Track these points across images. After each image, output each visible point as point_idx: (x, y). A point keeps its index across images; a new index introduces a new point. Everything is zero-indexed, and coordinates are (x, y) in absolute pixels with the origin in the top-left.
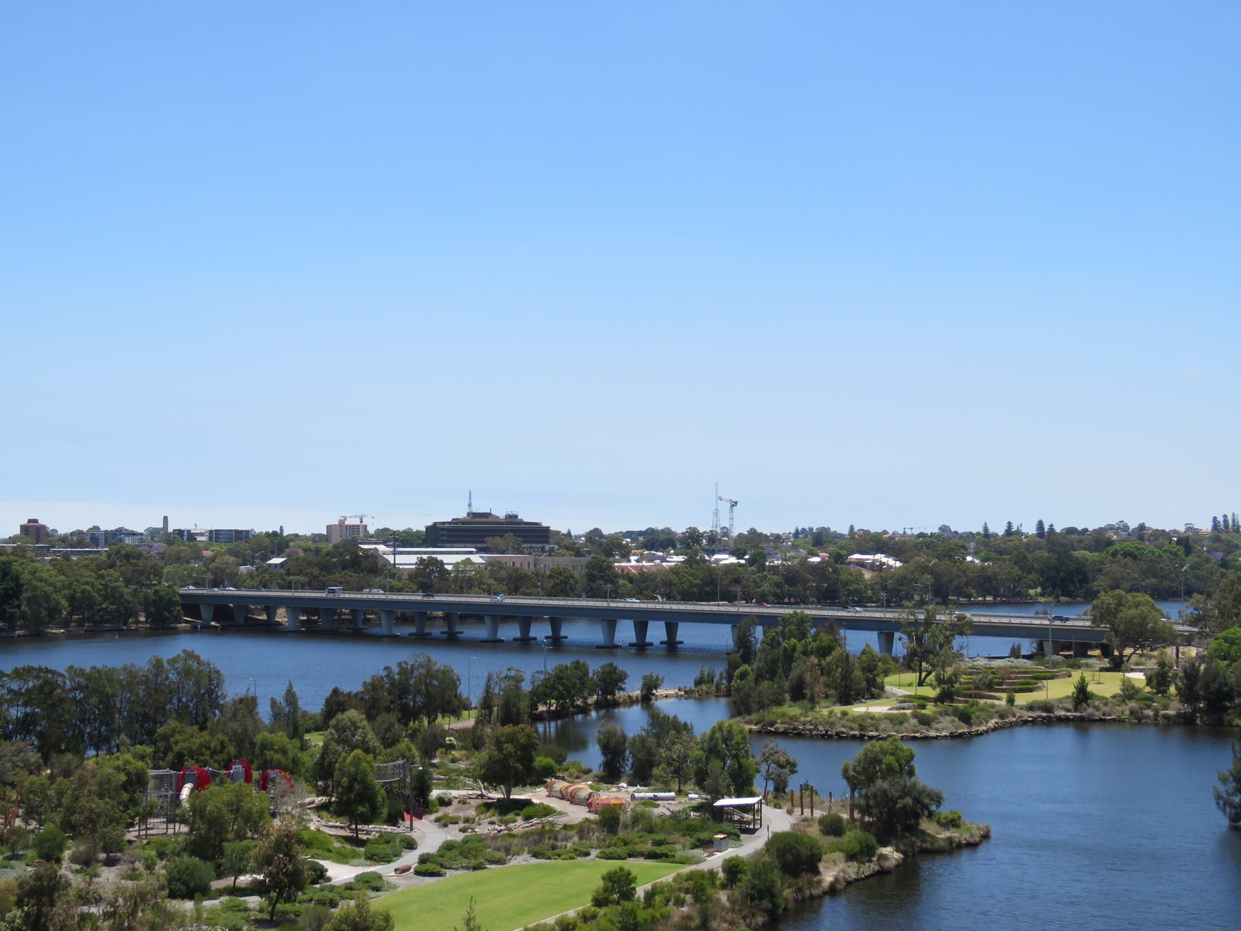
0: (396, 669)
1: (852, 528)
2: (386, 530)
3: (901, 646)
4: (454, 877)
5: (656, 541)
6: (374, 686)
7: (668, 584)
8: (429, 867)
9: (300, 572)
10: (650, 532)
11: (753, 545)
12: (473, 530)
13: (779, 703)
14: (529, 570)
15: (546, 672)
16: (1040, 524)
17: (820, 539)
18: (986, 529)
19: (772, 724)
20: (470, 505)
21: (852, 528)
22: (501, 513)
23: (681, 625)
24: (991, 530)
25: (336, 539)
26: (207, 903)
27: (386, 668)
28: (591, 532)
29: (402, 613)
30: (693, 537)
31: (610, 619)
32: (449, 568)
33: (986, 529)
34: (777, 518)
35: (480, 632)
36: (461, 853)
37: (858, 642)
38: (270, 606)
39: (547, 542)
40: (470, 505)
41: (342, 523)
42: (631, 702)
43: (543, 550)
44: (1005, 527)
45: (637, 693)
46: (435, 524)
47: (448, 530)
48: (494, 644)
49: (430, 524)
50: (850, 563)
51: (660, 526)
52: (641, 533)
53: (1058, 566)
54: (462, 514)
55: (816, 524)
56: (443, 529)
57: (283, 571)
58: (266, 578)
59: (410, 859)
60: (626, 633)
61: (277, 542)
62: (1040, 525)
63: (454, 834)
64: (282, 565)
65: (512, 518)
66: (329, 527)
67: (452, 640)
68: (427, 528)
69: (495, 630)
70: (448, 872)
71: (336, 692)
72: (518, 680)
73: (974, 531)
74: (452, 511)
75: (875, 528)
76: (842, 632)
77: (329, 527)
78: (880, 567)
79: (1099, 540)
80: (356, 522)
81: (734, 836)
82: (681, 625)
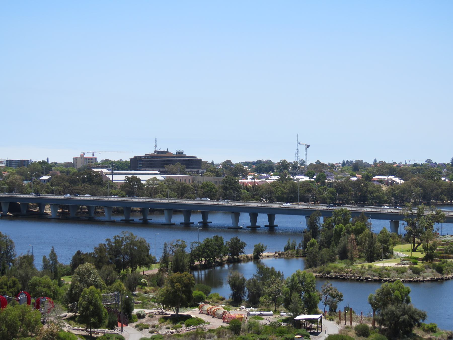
0: (113, 240)
1: (375, 160)
2: (107, 160)
3: (403, 228)
5: (262, 167)
6: (101, 250)
7: (269, 192)
9: (58, 185)
10: (259, 162)
11: (319, 170)
13: (333, 261)
14: (189, 184)
15: (199, 243)
17: (357, 167)
19: (329, 273)
20: (156, 146)
21: (375, 160)
22: (173, 151)
23: (276, 215)
25: (79, 166)
28: (225, 162)
30: (284, 165)
31: (236, 212)
32: (144, 182)
34: (332, 157)
35: (162, 219)
37: (378, 227)
38: (41, 204)
39: (200, 168)
40: (156, 146)
41: (82, 156)
42: (248, 259)
43: (198, 172)
45: (251, 254)
46: (136, 157)
47: (143, 161)
48: (169, 226)
49: (133, 157)
50: (374, 181)
52: (254, 163)
54: (151, 151)
55: (354, 158)
56: (141, 160)
58: (39, 188)
61: (45, 167)
64: (48, 180)
65: (180, 154)
66: (75, 159)
67: (145, 224)
68: (131, 160)
69: (170, 218)
71: (78, 253)
72: (183, 247)
73: (446, 163)
74: (145, 150)
75: (389, 160)
76: (369, 220)
77: (75, 159)
80: (90, 156)
82: (276, 215)
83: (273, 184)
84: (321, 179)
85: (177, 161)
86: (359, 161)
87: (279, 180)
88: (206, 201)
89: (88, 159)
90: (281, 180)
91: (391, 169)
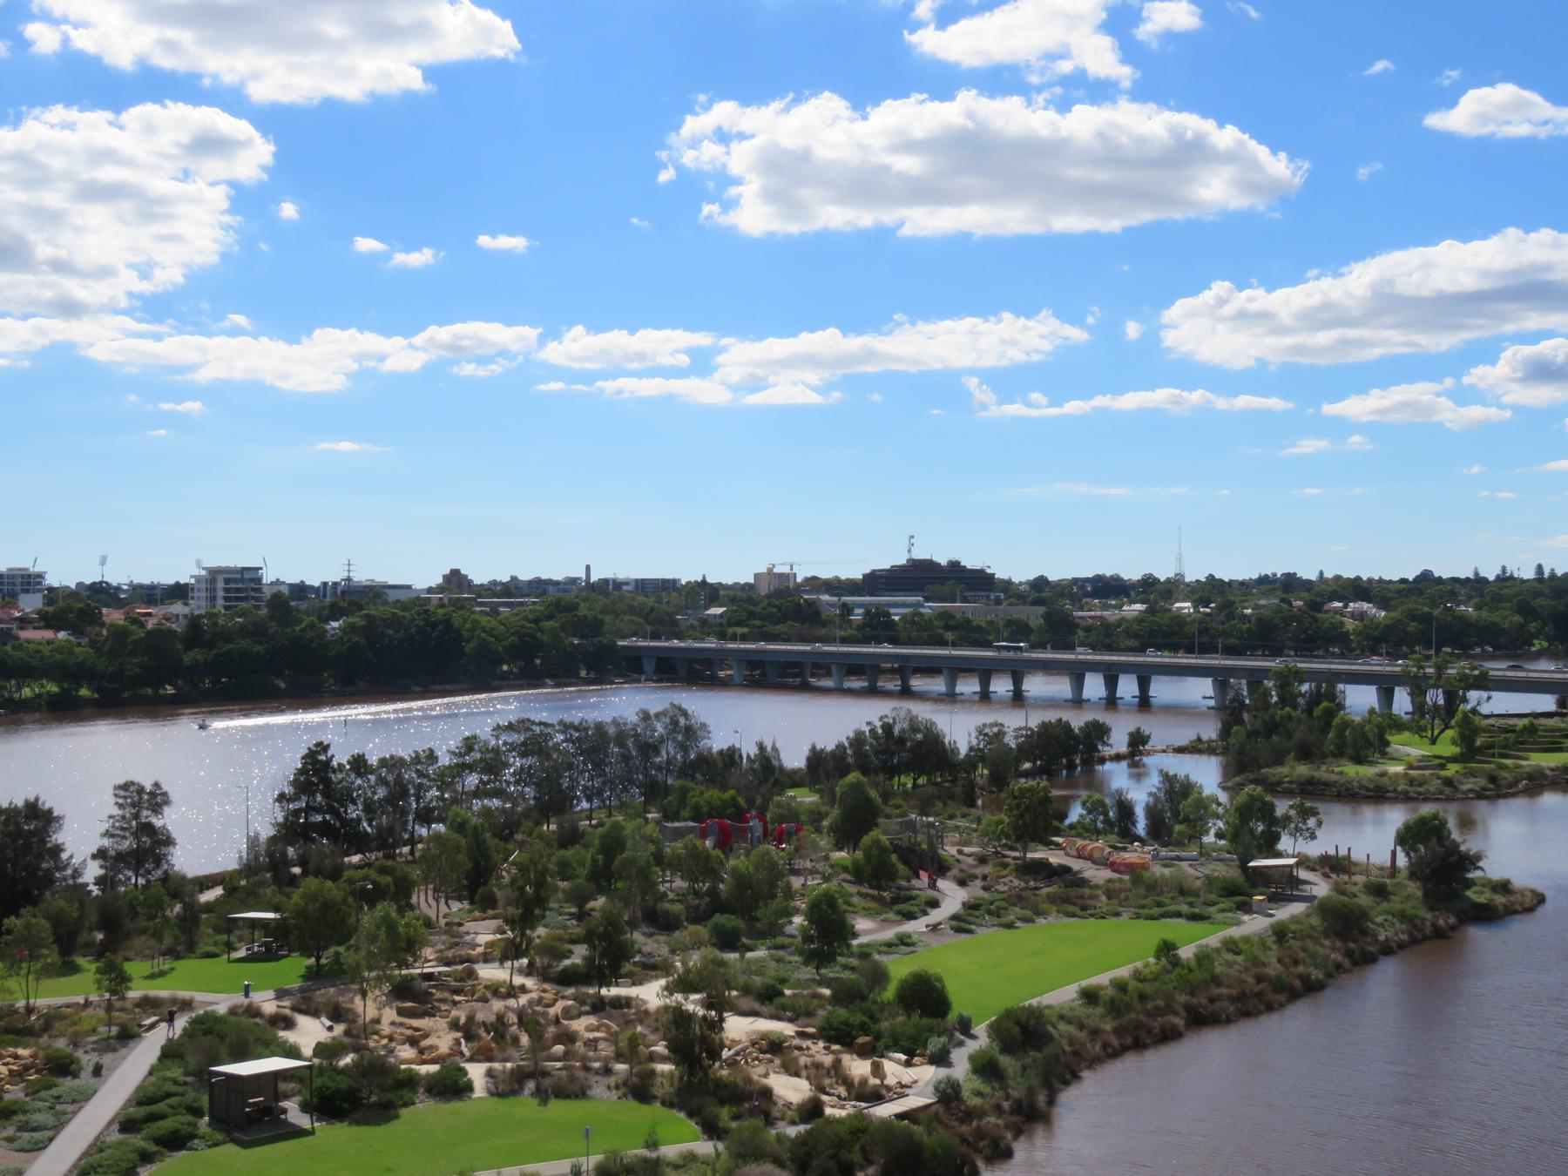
0: (878, 724)
1: (1321, 573)
2: (814, 578)
4: (989, 935)
5: (1109, 588)
6: (858, 741)
7: (1130, 634)
8: (962, 923)
9: (739, 624)
10: (1098, 579)
11: (1212, 589)
12: (917, 576)
13: (1279, 762)
14: (979, 620)
15: (1026, 728)
16: (1540, 567)
17: (1290, 583)
18: (1476, 574)
21: (1321, 573)
24: (1482, 574)
25: (763, 591)
26: (749, 955)
27: (869, 723)
29: (854, 668)
30: (1149, 583)
31: (1077, 674)
33: (1476, 574)
34: (1239, 564)
35: (938, 685)
36: (990, 913)
37: (1360, 699)
41: (770, 571)
42: (1118, 758)
43: (988, 597)
44: (1498, 571)
46: (873, 572)
48: (951, 697)
51: (1108, 572)
52: (1087, 580)
54: (901, 560)
55: (1279, 568)
56: (881, 577)
57: (724, 621)
58: (705, 627)
59: (936, 916)
60: (1094, 686)
61: (707, 592)
62: (1540, 568)
63: (975, 891)
64: (721, 616)
65: (955, 566)
66: (756, 576)
67: (906, 693)
68: (865, 576)
69: (952, 684)
70: (979, 930)
71: (813, 749)
72: (1000, 734)
73: (1463, 576)
74: (891, 557)
75: (1349, 574)
76: (1340, 686)
77: (756, 576)
78: (1361, 616)
80: (786, 570)
81: (1277, 899)
83: (1139, 620)
84: (1228, 608)
85: (948, 579)
86: (1289, 575)
87: (1145, 612)
89: (781, 575)
90: (1149, 611)
91: (1358, 589)
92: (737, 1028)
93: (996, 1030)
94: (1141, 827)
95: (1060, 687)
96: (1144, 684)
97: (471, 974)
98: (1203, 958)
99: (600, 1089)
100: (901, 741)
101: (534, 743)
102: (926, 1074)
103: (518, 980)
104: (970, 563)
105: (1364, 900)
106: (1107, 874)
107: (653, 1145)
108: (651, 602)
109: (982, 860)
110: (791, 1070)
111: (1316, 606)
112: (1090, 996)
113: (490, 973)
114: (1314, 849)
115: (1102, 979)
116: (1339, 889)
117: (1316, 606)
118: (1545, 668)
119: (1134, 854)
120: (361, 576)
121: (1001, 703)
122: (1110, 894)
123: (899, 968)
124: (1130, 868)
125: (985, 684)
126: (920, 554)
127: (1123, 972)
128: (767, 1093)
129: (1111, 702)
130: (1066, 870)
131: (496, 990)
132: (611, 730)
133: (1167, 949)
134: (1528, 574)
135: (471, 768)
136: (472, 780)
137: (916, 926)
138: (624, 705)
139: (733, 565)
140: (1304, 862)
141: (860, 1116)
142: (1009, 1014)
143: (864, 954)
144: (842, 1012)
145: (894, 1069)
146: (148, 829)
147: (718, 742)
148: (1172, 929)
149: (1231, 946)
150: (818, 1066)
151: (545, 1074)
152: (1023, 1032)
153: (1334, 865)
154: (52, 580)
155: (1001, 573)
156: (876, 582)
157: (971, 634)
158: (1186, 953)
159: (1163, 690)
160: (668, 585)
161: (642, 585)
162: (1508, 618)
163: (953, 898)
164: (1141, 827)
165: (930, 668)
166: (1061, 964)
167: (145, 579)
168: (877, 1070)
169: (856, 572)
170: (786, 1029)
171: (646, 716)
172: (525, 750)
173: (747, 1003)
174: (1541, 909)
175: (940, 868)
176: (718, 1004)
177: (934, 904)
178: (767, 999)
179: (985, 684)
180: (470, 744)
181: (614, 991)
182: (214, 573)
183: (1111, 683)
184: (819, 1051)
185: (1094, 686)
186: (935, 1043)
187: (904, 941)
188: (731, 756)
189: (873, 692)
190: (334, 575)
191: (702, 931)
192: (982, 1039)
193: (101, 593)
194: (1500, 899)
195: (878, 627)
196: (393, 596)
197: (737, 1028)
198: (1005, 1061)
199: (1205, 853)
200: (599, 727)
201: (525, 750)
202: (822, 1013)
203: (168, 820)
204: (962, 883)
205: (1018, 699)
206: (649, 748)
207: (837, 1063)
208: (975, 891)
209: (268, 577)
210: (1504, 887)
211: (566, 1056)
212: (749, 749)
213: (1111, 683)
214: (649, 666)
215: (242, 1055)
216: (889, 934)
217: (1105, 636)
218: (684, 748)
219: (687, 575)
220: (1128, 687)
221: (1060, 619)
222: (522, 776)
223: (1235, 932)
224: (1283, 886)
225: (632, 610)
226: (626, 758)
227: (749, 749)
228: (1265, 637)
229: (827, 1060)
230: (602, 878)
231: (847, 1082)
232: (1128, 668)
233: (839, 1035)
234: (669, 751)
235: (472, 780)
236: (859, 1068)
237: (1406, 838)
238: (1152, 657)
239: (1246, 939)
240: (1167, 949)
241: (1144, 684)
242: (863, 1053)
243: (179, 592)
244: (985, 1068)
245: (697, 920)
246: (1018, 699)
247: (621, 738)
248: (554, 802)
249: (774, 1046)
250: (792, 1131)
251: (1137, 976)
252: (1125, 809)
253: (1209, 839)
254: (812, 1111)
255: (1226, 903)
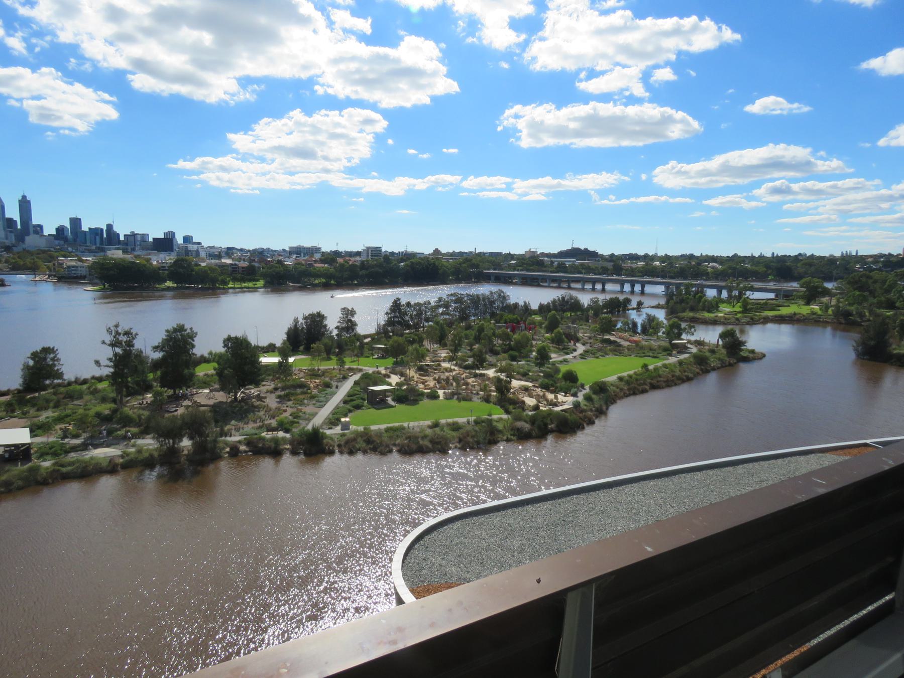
3: (725, 294)
4: (591, 360)
5: (634, 257)
6: (554, 302)
7: (639, 272)
8: (583, 356)
10: (630, 254)
11: (666, 258)
12: (575, 253)
13: (684, 312)
14: (593, 267)
17: (691, 257)
29: (554, 280)
30: (646, 257)
31: (622, 283)
34: (675, 251)
35: (579, 286)
37: (711, 293)
38: (514, 276)
42: (633, 309)
45: (635, 306)
48: (583, 290)
53: (781, 268)
54: (570, 248)
55: (688, 252)
58: (511, 267)
59: (575, 354)
60: (627, 287)
61: (510, 256)
63: (588, 347)
67: (569, 288)
69: (583, 286)
78: (713, 267)
79: (798, 258)
81: (680, 353)
83: (643, 267)
84: (671, 264)
88: (604, 276)
91: (713, 259)
92: (515, 383)
93: (591, 387)
94: (639, 330)
95: (617, 287)
96: (643, 287)
97: (439, 365)
98: (656, 369)
99: (475, 398)
100: (567, 302)
101: (459, 300)
102: (570, 399)
103: (453, 367)
104: (591, 249)
105: (708, 354)
106: (628, 343)
107: (490, 415)
108: (494, 259)
109: (590, 338)
110: (531, 396)
111: (699, 264)
112: (621, 379)
113: (445, 365)
114: (693, 338)
115: (625, 374)
116: (700, 351)
117: (699, 264)
118: (771, 285)
119: (637, 338)
120: (410, 250)
121: (598, 292)
122: (629, 349)
123: (564, 368)
124: (635, 342)
125: (594, 286)
126: (575, 246)
127: (631, 372)
128: (523, 402)
129: (632, 292)
130: (615, 342)
131: (446, 370)
132: (481, 297)
133: (645, 366)
134: (769, 255)
135: (440, 306)
136: (441, 310)
137: (568, 357)
138: (484, 290)
139: (519, 249)
140: (689, 342)
141: (550, 410)
142: (596, 384)
143: (553, 364)
144: (546, 380)
145: (561, 397)
146: (350, 321)
147: (512, 301)
148: (647, 360)
149: (665, 366)
150: (538, 395)
151: (460, 394)
152: (600, 388)
153: (699, 343)
154: (323, 250)
155: (600, 252)
156: (561, 254)
157: (589, 270)
158: (651, 367)
159: (649, 289)
160: (499, 254)
161: (491, 254)
162: (761, 269)
163: (581, 348)
164: (639, 330)
165: (577, 281)
166: (613, 369)
167: (349, 250)
168: (556, 397)
169: (555, 250)
170: (530, 384)
171: (491, 293)
172: (456, 302)
173: (519, 377)
174: (764, 359)
175: (577, 340)
176: (510, 377)
177: (575, 350)
178: (524, 376)
179: (594, 286)
180: (440, 299)
181: (481, 372)
182: (368, 248)
183: (633, 286)
184: (539, 391)
185: (627, 287)
186: (573, 391)
187: (565, 361)
188: (516, 305)
189: (559, 287)
190: (402, 250)
191: (506, 355)
192: (587, 390)
193: (337, 254)
194: (751, 355)
195: (562, 268)
196: (419, 256)
197: (515, 383)
198: (594, 396)
199: (658, 338)
200: (478, 296)
201: (456, 302)
202: (540, 381)
203: (355, 319)
204: (584, 344)
205: (603, 290)
206: (492, 302)
207: (544, 395)
208: (588, 347)
209: (383, 250)
210: (753, 352)
211: (466, 389)
212: (521, 303)
213: (633, 286)
214: (493, 278)
215: (376, 385)
216: (561, 358)
217: (632, 272)
218: (502, 303)
219: (505, 251)
220: (638, 288)
221: (616, 267)
222: (456, 308)
223: (666, 362)
224: (683, 349)
225: (488, 261)
226: (485, 305)
227: (521, 303)
228: (682, 273)
229: (541, 394)
230: (477, 339)
231: (547, 400)
232: (638, 282)
233: (545, 387)
234: (498, 303)
235: (441, 310)
236: (550, 396)
237: (722, 336)
238: (646, 279)
239: (670, 364)
240: (645, 366)
241: (643, 287)
242: (552, 392)
243: (358, 254)
244: (588, 398)
245: (504, 352)
246: (603, 290)
247: (484, 300)
248: (464, 317)
249: (526, 389)
250: (530, 413)
251: (635, 373)
252: (635, 325)
253: (660, 334)
254: (536, 408)
255: (664, 353)
